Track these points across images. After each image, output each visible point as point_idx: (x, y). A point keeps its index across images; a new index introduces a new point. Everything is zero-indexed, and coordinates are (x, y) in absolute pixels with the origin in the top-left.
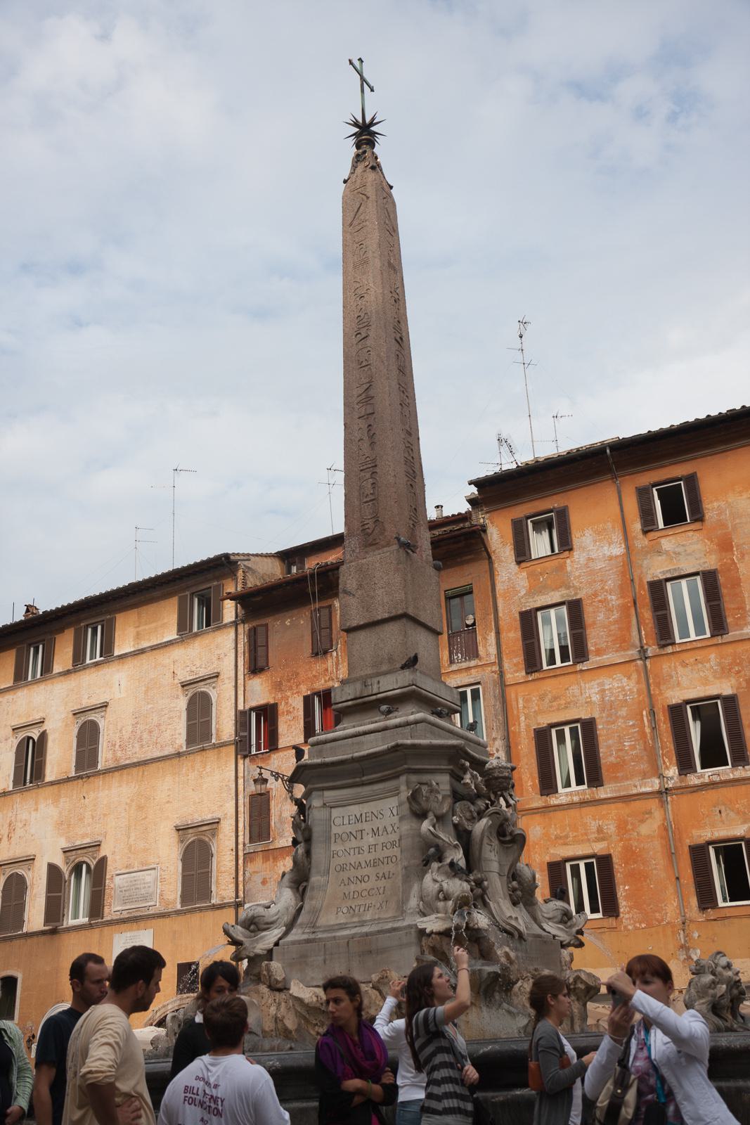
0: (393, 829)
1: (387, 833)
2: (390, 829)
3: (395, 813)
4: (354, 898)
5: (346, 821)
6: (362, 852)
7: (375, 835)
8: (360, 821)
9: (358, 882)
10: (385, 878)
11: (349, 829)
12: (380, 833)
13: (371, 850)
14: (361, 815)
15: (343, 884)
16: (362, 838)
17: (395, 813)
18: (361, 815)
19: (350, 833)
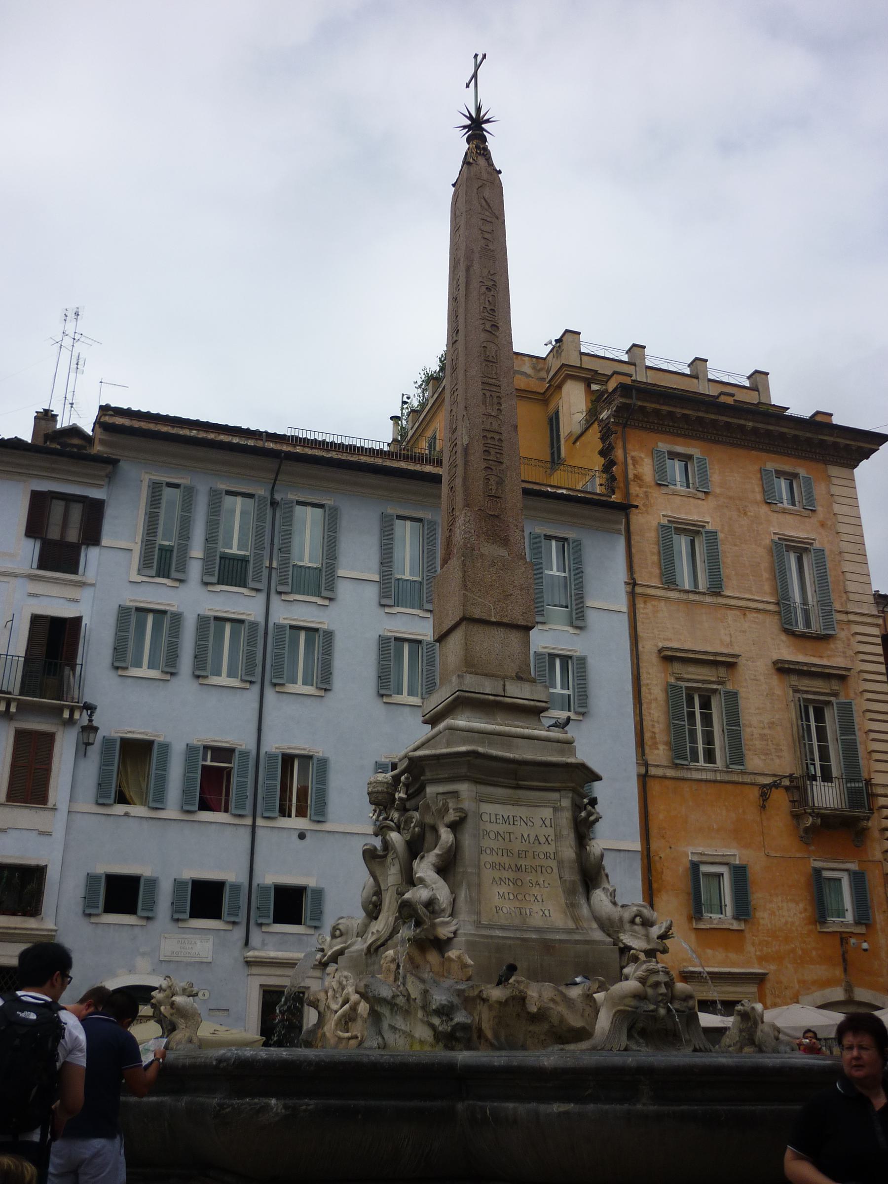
0: (547, 839)
1: (540, 843)
2: (542, 840)
3: (548, 822)
4: (509, 899)
5: (493, 819)
6: (511, 855)
7: (525, 841)
8: (507, 822)
9: (511, 884)
10: (540, 887)
11: (496, 828)
12: (532, 841)
13: (520, 856)
14: (509, 816)
15: (494, 883)
16: (510, 841)
17: (548, 822)
18: (509, 816)
19: (498, 832)
